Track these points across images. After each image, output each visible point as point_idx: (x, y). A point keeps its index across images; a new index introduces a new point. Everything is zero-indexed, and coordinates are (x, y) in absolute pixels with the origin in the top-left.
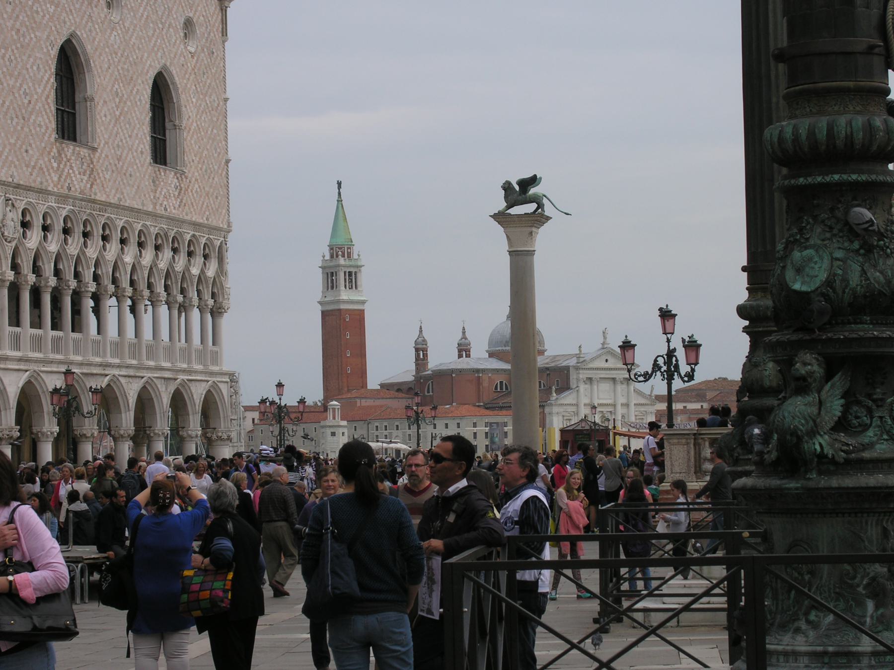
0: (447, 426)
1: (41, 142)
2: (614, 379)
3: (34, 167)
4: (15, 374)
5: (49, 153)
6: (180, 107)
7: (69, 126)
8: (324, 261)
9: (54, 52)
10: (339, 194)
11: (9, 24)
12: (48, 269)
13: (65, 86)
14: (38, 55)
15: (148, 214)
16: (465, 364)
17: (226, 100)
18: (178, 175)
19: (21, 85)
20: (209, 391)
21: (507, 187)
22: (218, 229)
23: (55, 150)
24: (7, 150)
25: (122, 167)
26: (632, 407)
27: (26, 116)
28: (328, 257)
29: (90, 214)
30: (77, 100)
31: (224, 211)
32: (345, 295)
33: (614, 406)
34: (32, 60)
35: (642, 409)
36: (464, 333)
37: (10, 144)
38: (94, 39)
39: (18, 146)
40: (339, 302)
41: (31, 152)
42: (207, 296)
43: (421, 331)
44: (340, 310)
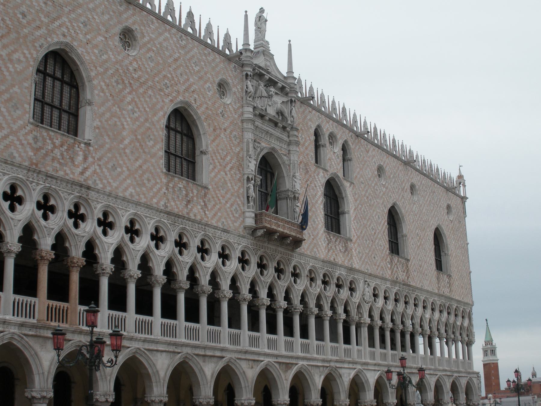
1: (382, 254)
3: (378, 266)
4: (373, 372)
5: (386, 260)
6: (447, 244)
7: (395, 247)
9: (386, 211)
11: (363, 193)
12: (388, 318)
13: (392, 230)
14: (378, 211)
15: (436, 294)
17: (468, 244)
19: (370, 224)
20: (468, 382)
23: (389, 259)
24: (364, 256)
27: (374, 240)
28: (484, 345)
29: (408, 292)
30: (398, 237)
34: (375, 213)
37: (366, 253)
38: (405, 207)
39: (370, 254)
41: (376, 258)
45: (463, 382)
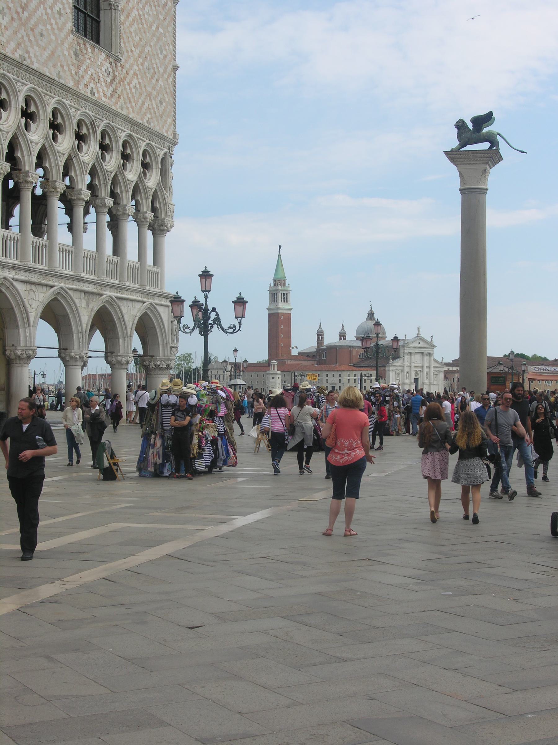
0: (333, 375)
2: (423, 353)
8: (270, 287)
10: (279, 252)
15: (67, 89)
16: (343, 343)
18: (112, 60)
20: (145, 314)
21: (460, 126)
22: (163, 138)
25: (29, 19)
26: (432, 369)
28: (272, 285)
31: (169, 121)
32: (281, 305)
33: (423, 367)
35: (437, 369)
36: (343, 327)
40: (278, 309)
42: (146, 208)
43: (320, 326)
44: (278, 313)
45: (130, 314)
